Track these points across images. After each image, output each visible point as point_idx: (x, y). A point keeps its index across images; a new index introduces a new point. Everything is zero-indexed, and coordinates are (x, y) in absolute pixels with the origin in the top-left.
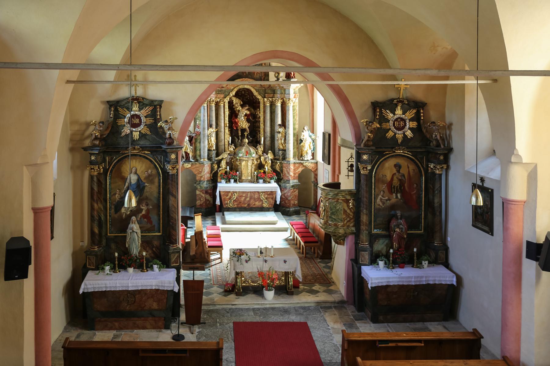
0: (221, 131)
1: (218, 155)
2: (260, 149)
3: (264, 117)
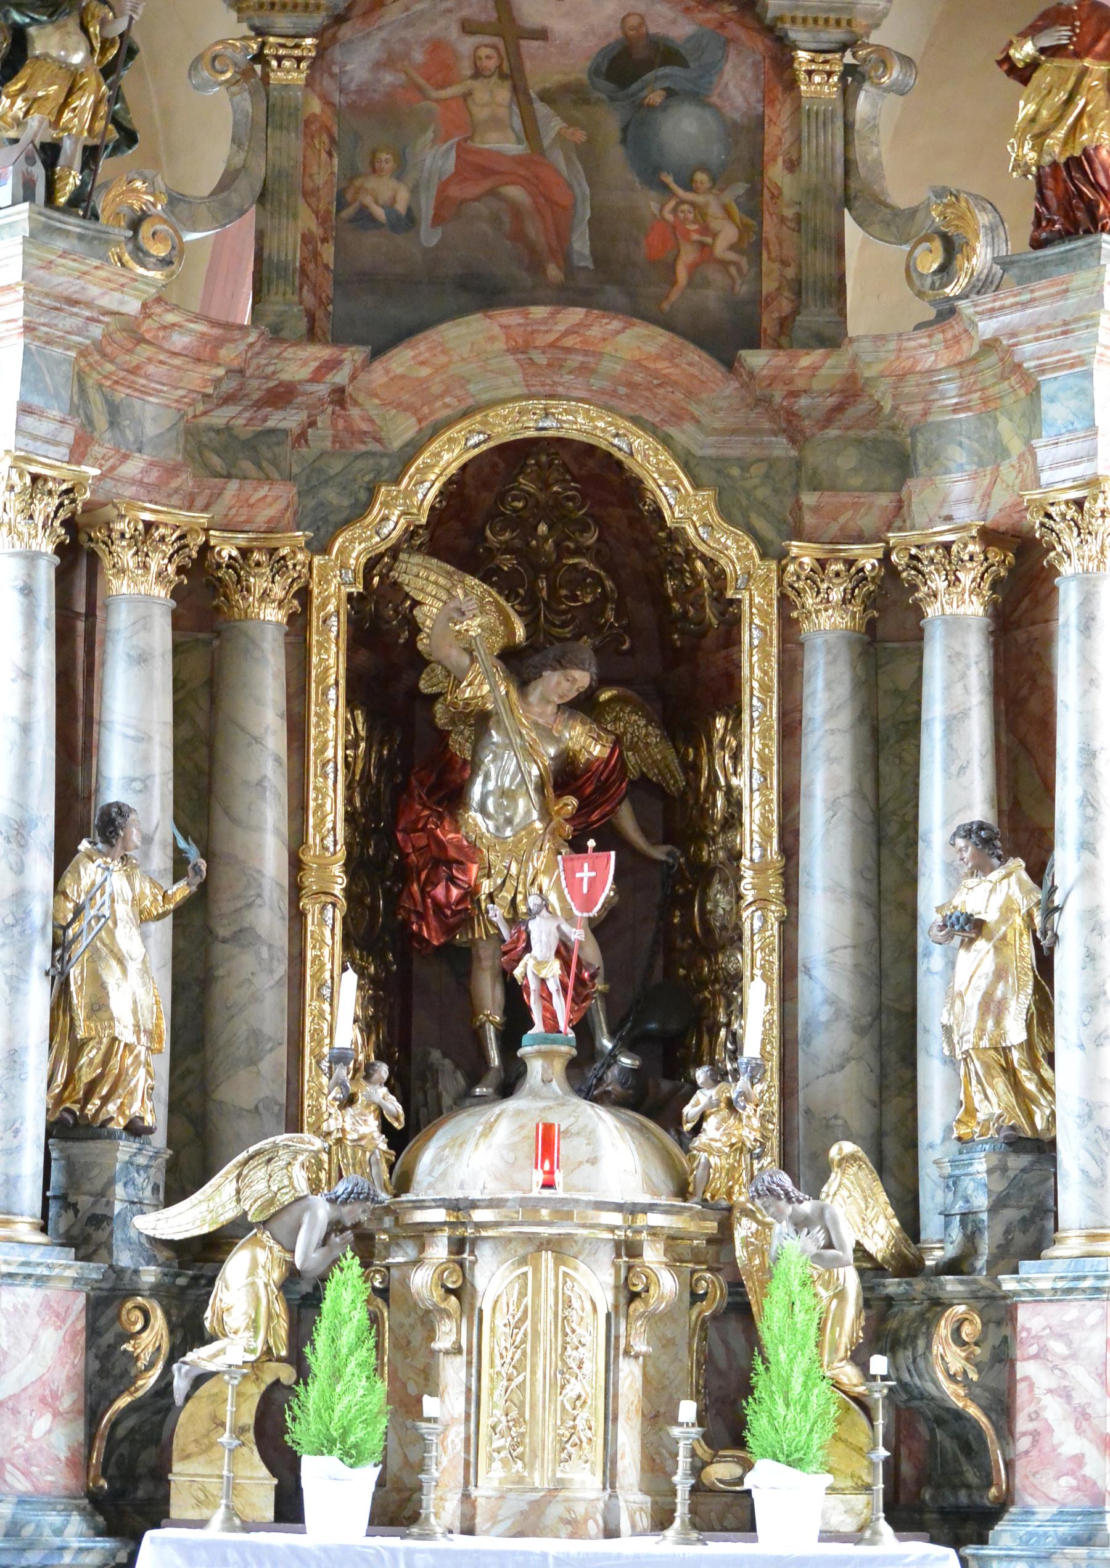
0: (244, 936)
1: (180, 1183)
2: (729, 1120)
3: (790, 797)
